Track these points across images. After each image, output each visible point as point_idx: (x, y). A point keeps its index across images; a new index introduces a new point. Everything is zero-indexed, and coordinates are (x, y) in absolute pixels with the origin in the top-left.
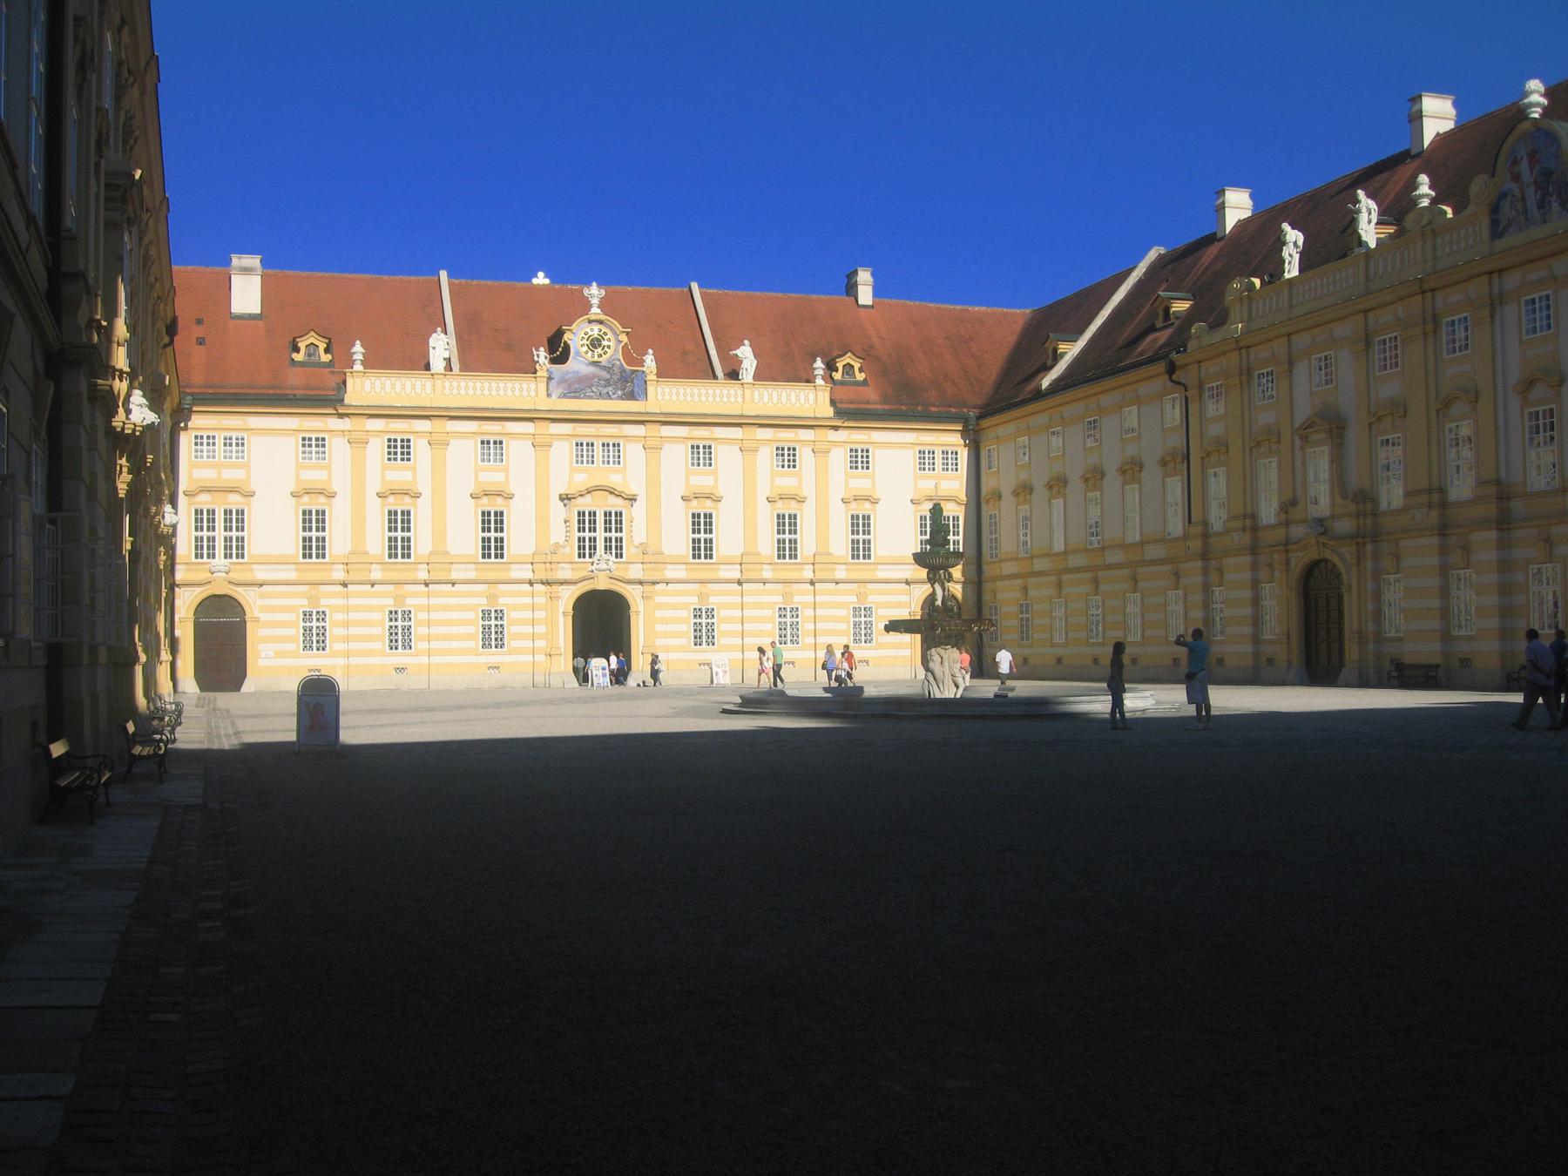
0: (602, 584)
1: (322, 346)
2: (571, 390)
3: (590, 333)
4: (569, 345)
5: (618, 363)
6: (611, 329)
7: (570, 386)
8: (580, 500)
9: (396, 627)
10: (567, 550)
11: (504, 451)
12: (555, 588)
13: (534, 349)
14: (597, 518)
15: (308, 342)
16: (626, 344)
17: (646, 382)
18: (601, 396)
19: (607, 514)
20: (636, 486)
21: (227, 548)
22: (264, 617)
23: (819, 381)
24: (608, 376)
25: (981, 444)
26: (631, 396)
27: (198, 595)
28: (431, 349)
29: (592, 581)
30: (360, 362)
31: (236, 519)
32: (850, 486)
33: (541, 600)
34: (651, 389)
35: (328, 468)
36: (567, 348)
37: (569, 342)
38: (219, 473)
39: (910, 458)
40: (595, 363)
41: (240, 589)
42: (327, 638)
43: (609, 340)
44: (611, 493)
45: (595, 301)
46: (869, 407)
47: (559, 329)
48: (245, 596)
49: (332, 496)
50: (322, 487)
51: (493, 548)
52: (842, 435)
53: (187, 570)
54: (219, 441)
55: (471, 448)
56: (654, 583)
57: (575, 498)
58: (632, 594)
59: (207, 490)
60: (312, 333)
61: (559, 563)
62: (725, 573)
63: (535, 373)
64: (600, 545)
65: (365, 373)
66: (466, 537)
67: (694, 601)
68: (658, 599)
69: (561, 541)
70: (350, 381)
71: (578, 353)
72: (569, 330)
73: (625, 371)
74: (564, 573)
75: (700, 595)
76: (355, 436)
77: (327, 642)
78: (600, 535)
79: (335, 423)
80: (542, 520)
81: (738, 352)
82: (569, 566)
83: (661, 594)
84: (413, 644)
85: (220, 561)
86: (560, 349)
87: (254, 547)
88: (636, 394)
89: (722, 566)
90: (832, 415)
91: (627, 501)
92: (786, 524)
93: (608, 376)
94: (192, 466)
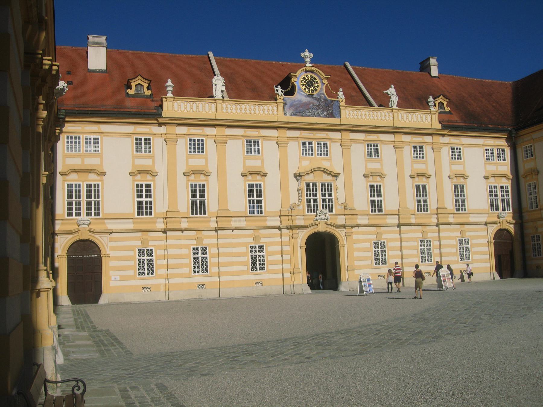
0: (323, 228)
1: (146, 85)
2: (297, 111)
4: (295, 84)
5: (323, 96)
6: (318, 76)
7: (296, 109)
8: (307, 177)
9: (198, 258)
10: (301, 208)
11: (260, 147)
12: (295, 231)
15: (137, 83)
16: (327, 85)
17: (339, 107)
18: (314, 115)
19: (323, 185)
21: (89, 209)
22: (113, 254)
25: (516, 145)
26: (331, 115)
27: (70, 240)
28: (214, 85)
29: (317, 226)
30: (170, 92)
32: (452, 169)
33: (286, 239)
34: (343, 111)
35: (153, 157)
36: (293, 87)
37: (295, 83)
38: (83, 161)
41: (97, 236)
42: (154, 267)
43: (317, 82)
44: (325, 172)
45: (308, 60)
46: (458, 124)
47: (288, 75)
48: (101, 240)
49: (155, 175)
52: (446, 140)
53: (62, 224)
54: (83, 140)
56: (352, 227)
57: (304, 175)
58: (340, 234)
59: (75, 171)
60: (139, 77)
63: (276, 101)
65: (174, 98)
68: (355, 237)
70: (165, 104)
71: (300, 89)
74: (300, 222)
75: (377, 234)
77: (154, 269)
79: (156, 129)
80: (284, 189)
81: (388, 91)
82: (302, 217)
83: (358, 234)
84: (208, 269)
85: (84, 217)
86: (290, 87)
87: (106, 207)
88: (334, 114)
89: (388, 216)
92: (421, 191)
93: (318, 104)
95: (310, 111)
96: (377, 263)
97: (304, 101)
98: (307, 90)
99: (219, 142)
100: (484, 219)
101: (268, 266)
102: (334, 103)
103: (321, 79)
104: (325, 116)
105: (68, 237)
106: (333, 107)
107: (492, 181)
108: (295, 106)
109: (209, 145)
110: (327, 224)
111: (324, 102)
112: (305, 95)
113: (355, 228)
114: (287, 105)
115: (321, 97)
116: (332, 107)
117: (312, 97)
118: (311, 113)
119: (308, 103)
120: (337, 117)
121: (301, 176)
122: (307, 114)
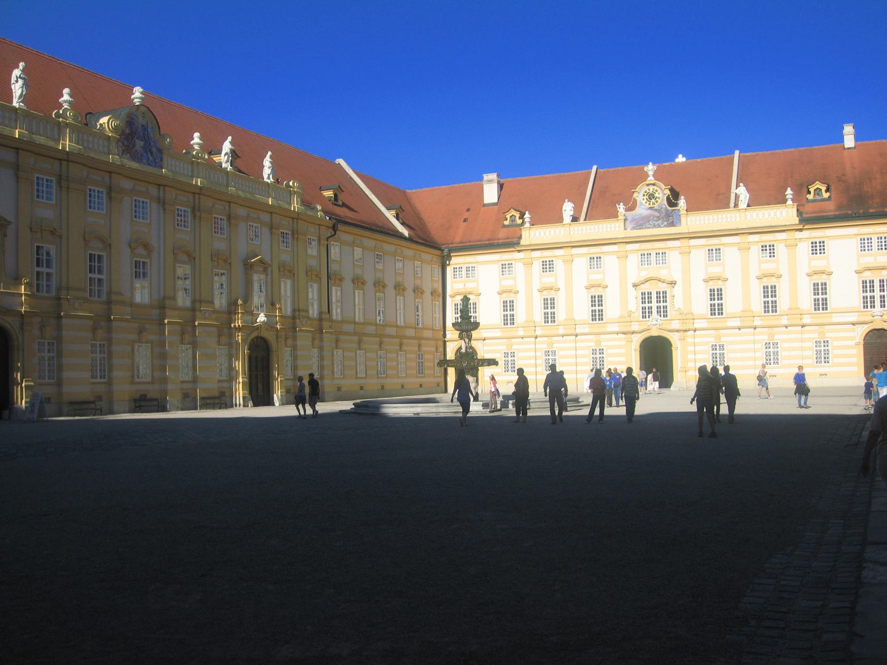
0: (655, 333)
3: (648, 191)
4: (636, 200)
6: (660, 187)
7: (637, 223)
8: (642, 286)
10: (636, 314)
12: (629, 336)
13: (617, 205)
14: (652, 296)
15: (511, 215)
16: (669, 195)
17: (680, 215)
18: (655, 226)
20: (677, 276)
23: (789, 202)
26: (672, 224)
28: (563, 211)
34: (683, 219)
37: (637, 198)
39: (853, 245)
40: (651, 208)
45: (651, 173)
51: (597, 315)
52: (805, 234)
54: (464, 270)
55: (585, 261)
56: (685, 331)
57: (639, 285)
58: (674, 338)
61: (631, 322)
62: (731, 323)
64: (654, 310)
66: (583, 311)
67: (712, 341)
69: (634, 309)
71: (641, 204)
72: (635, 191)
73: (667, 210)
74: (635, 327)
78: (654, 305)
79: (517, 255)
82: (637, 323)
86: (631, 203)
88: (675, 223)
89: (728, 319)
90: (797, 222)
91: (669, 285)
93: (659, 215)
95: (651, 223)
99: (569, 261)
100: (854, 318)
103: (662, 190)
104: (666, 226)
107: (868, 276)
109: (559, 265)
110: (660, 329)
113: (690, 332)
114: (628, 221)
121: (636, 286)
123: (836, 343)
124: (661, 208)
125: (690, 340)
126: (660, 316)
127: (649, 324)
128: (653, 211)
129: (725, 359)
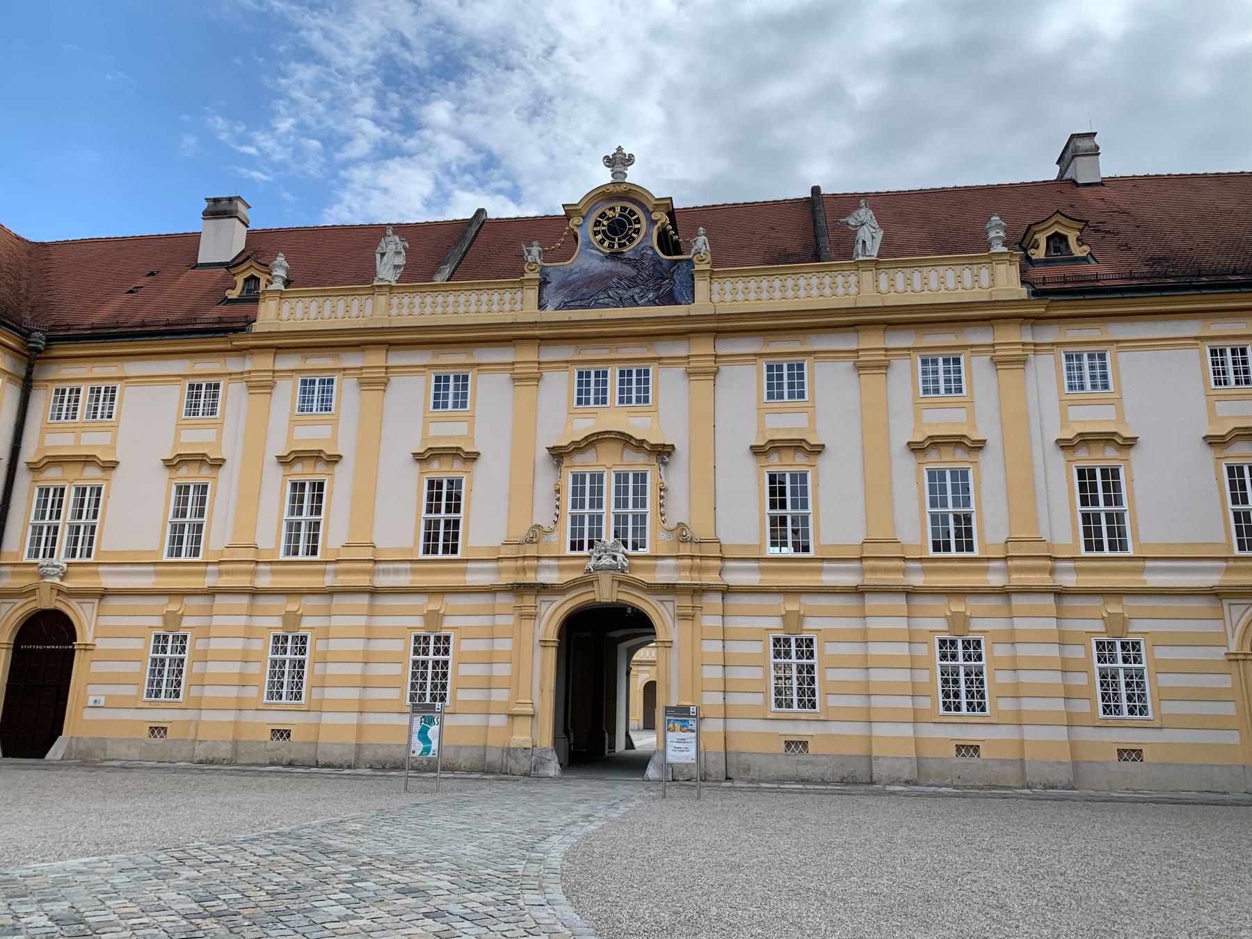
2: (575, 298)
7: (574, 292)
8: (578, 459)
10: (554, 538)
12: (529, 600)
18: (621, 302)
19: (621, 478)
22: (101, 644)
23: (999, 248)
24: (634, 273)
26: (670, 298)
28: (378, 256)
31: (90, 499)
34: (701, 286)
38: (78, 439)
41: (73, 603)
50: (201, 452)
54: (84, 396)
57: (569, 454)
73: (659, 262)
76: (255, 377)
79: (233, 365)
88: (676, 294)
93: (634, 273)
94: (46, 430)
96: (782, 701)
97: (597, 271)
98: (606, 244)
101: (454, 693)
102: (678, 267)
105: (16, 603)
106: (675, 277)
108: (570, 285)
111: (651, 268)
112: (601, 255)
115: (642, 255)
116: (672, 279)
117: (619, 259)
118: (612, 298)
119: (606, 275)
120: (683, 302)
122: (601, 301)
123: (1162, 653)
124: (642, 255)
125: (711, 621)
126: (625, 544)
127: (591, 564)
128: (619, 264)
129: (817, 686)
